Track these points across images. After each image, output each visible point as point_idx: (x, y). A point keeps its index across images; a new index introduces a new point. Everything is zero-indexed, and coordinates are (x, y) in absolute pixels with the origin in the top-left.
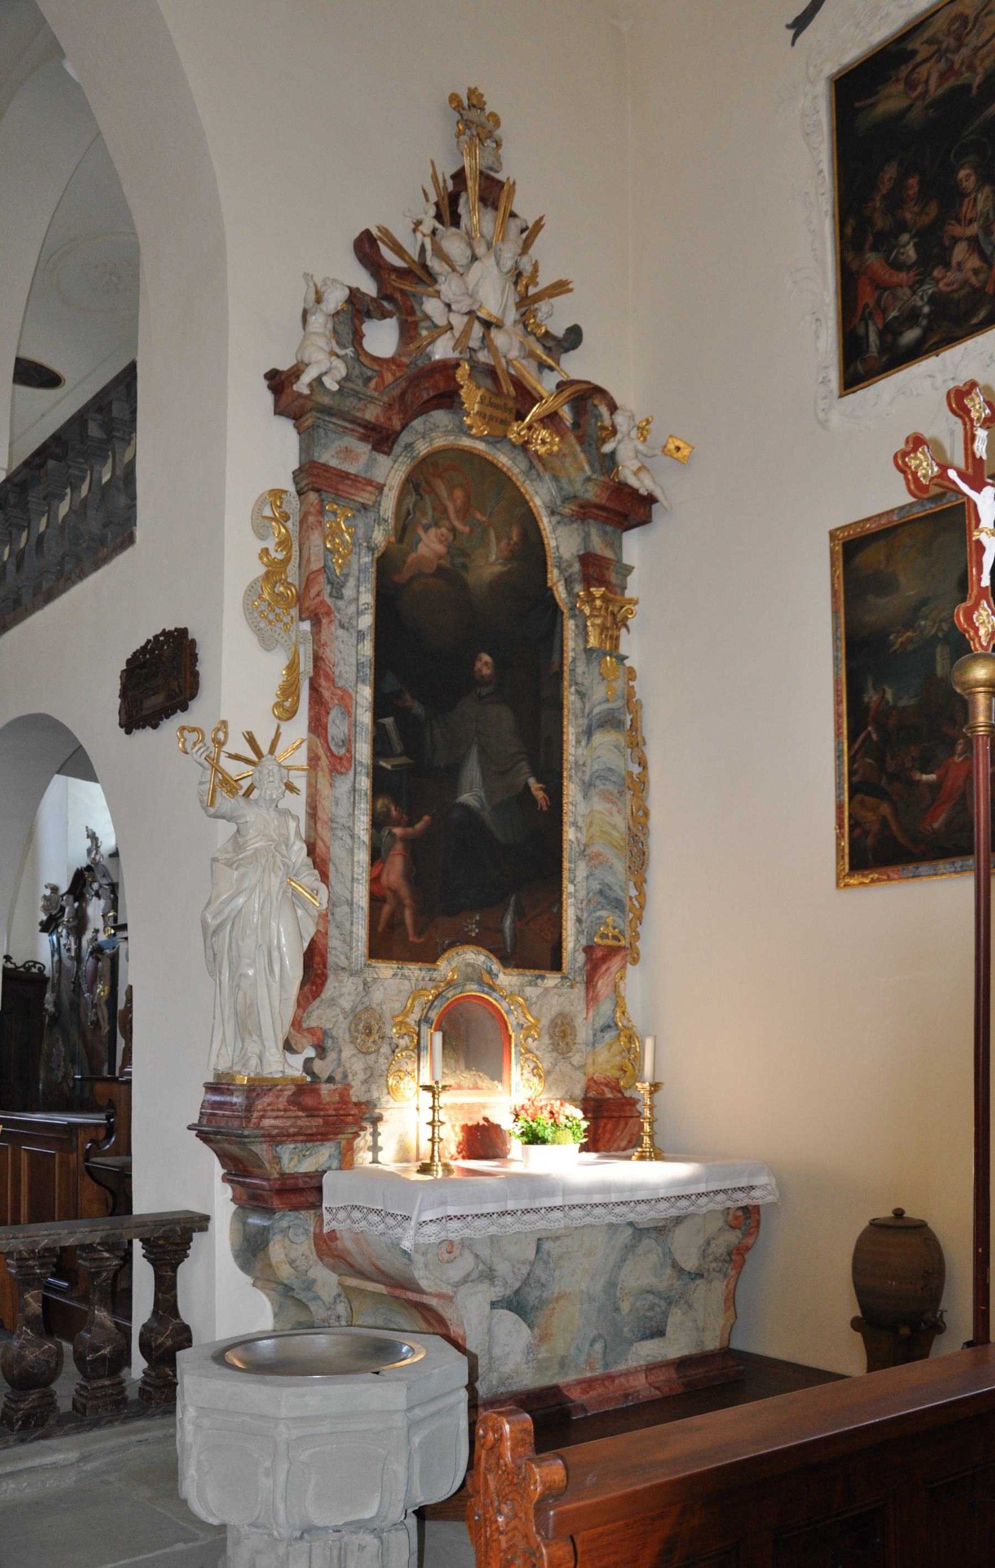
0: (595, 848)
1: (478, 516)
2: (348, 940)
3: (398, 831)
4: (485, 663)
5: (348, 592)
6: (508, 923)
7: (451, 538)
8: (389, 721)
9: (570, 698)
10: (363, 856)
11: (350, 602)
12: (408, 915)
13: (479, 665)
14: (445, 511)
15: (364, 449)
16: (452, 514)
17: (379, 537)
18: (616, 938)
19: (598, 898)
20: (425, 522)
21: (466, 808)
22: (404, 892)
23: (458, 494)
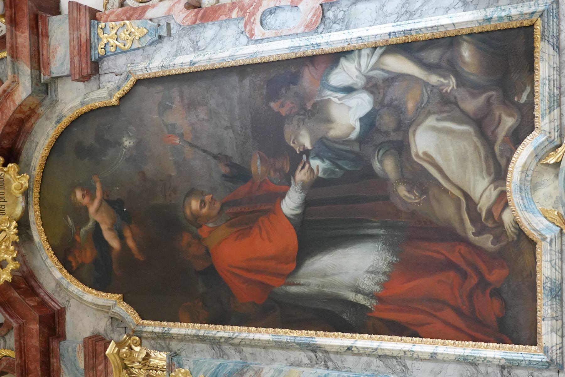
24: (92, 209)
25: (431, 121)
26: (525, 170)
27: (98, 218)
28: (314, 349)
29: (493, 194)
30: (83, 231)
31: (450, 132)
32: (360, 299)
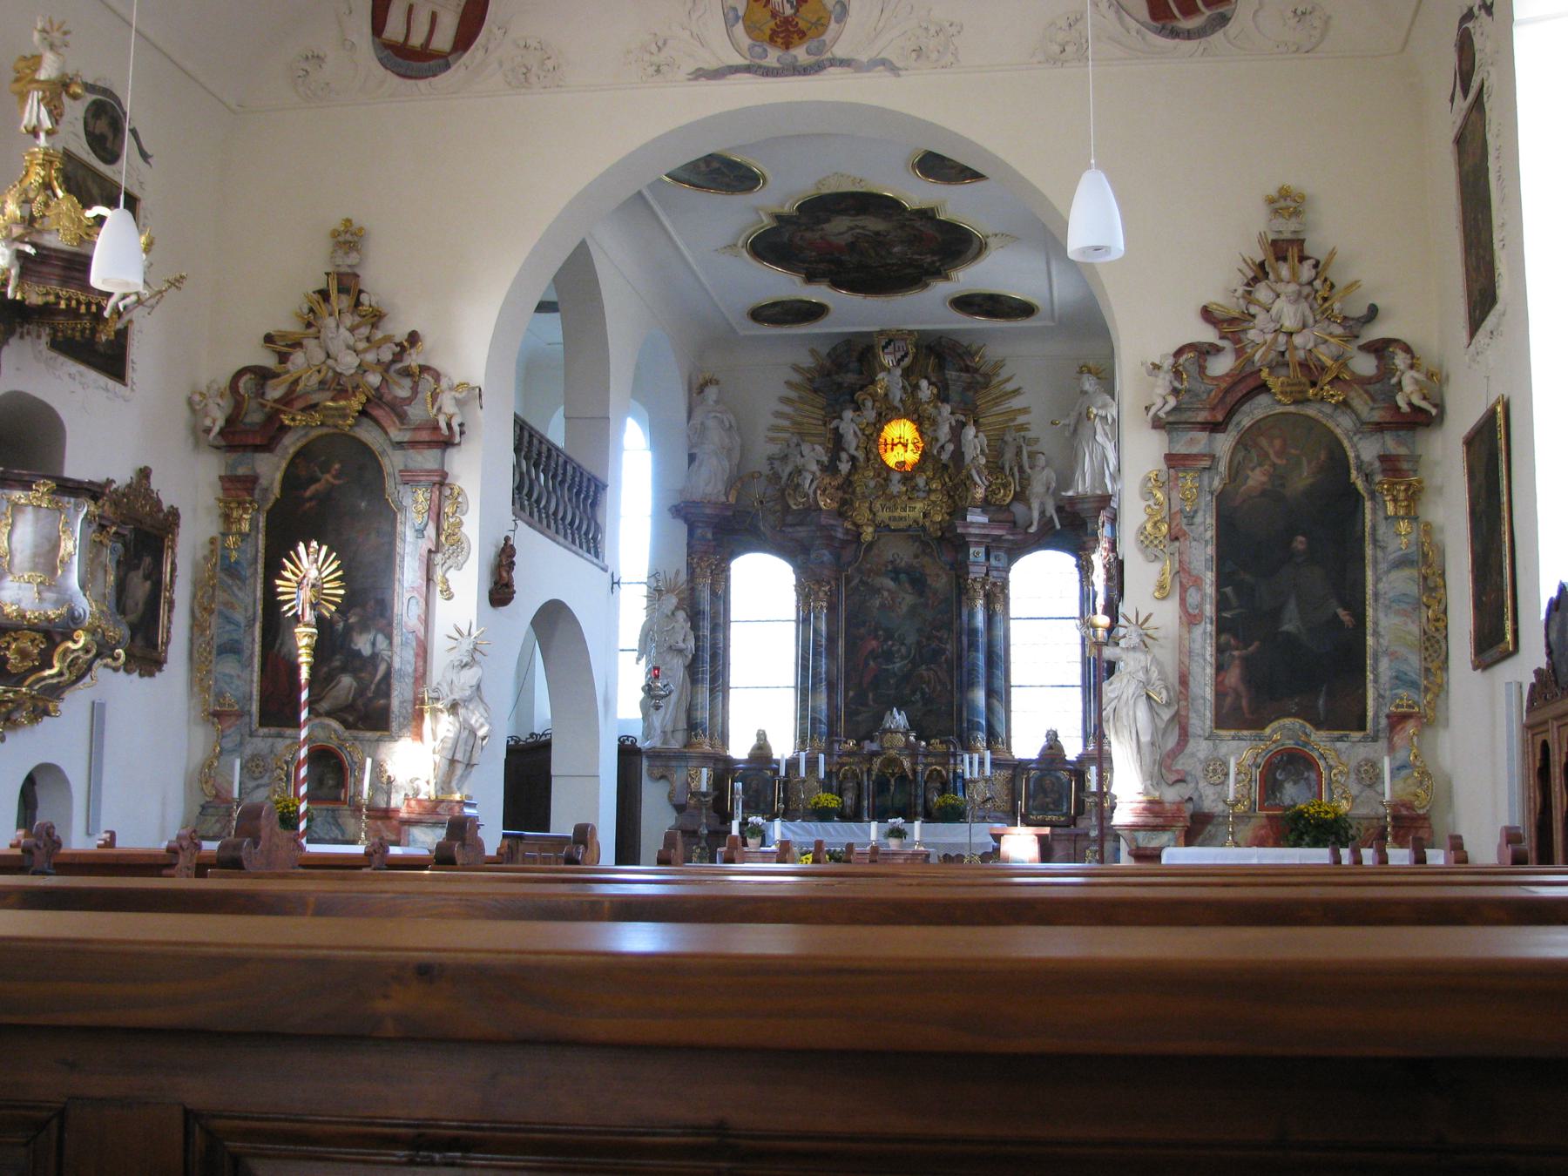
0: (1392, 649)
1: (1293, 451)
2: (1202, 718)
3: (1236, 653)
4: (1300, 542)
5: (1198, 519)
6: (1321, 702)
7: (1272, 470)
8: (1228, 590)
9: (1369, 551)
10: (1210, 671)
11: (1199, 525)
12: (1244, 703)
13: (1295, 544)
14: (1266, 455)
15: (1203, 436)
16: (1272, 456)
17: (1217, 484)
18: (1409, 706)
19: (1394, 681)
20: (1251, 465)
21: (1288, 633)
22: (1242, 688)
23: (1277, 443)
24: (328, 477)
25: (355, 684)
26: (328, 725)
27: (323, 481)
28: (254, 620)
29: (321, 711)
30: (316, 468)
31: (349, 693)
32: (277, 646)
